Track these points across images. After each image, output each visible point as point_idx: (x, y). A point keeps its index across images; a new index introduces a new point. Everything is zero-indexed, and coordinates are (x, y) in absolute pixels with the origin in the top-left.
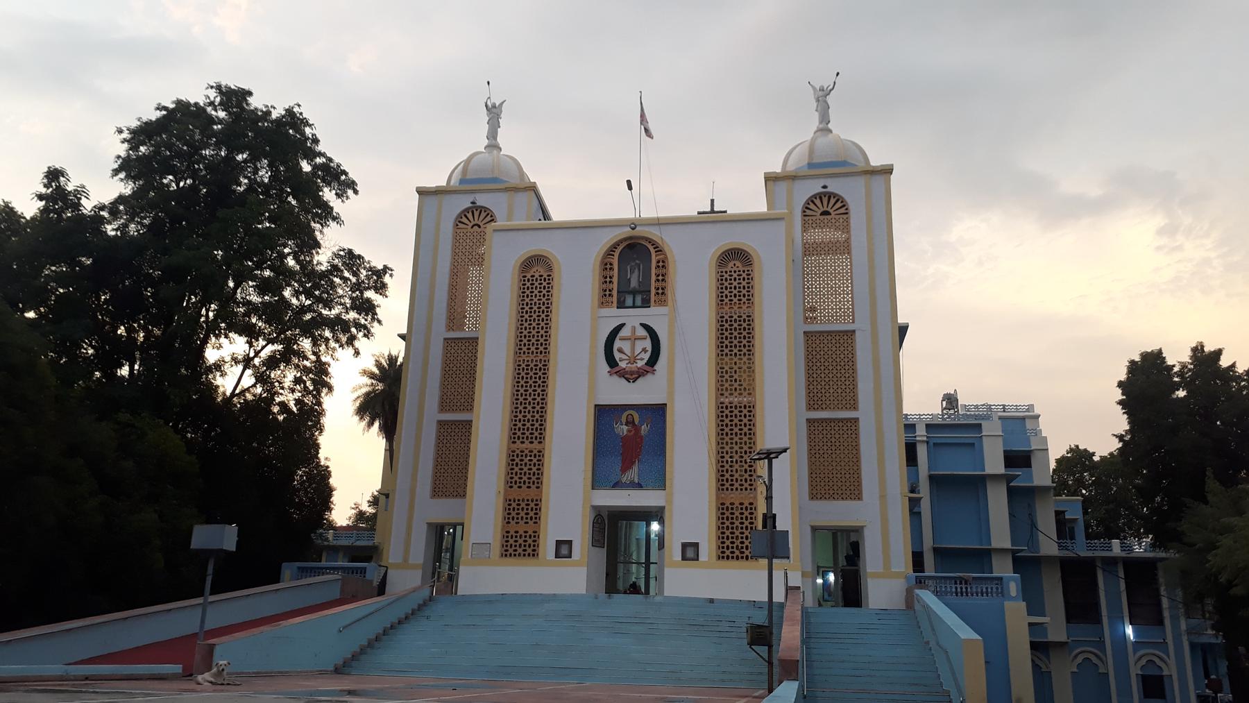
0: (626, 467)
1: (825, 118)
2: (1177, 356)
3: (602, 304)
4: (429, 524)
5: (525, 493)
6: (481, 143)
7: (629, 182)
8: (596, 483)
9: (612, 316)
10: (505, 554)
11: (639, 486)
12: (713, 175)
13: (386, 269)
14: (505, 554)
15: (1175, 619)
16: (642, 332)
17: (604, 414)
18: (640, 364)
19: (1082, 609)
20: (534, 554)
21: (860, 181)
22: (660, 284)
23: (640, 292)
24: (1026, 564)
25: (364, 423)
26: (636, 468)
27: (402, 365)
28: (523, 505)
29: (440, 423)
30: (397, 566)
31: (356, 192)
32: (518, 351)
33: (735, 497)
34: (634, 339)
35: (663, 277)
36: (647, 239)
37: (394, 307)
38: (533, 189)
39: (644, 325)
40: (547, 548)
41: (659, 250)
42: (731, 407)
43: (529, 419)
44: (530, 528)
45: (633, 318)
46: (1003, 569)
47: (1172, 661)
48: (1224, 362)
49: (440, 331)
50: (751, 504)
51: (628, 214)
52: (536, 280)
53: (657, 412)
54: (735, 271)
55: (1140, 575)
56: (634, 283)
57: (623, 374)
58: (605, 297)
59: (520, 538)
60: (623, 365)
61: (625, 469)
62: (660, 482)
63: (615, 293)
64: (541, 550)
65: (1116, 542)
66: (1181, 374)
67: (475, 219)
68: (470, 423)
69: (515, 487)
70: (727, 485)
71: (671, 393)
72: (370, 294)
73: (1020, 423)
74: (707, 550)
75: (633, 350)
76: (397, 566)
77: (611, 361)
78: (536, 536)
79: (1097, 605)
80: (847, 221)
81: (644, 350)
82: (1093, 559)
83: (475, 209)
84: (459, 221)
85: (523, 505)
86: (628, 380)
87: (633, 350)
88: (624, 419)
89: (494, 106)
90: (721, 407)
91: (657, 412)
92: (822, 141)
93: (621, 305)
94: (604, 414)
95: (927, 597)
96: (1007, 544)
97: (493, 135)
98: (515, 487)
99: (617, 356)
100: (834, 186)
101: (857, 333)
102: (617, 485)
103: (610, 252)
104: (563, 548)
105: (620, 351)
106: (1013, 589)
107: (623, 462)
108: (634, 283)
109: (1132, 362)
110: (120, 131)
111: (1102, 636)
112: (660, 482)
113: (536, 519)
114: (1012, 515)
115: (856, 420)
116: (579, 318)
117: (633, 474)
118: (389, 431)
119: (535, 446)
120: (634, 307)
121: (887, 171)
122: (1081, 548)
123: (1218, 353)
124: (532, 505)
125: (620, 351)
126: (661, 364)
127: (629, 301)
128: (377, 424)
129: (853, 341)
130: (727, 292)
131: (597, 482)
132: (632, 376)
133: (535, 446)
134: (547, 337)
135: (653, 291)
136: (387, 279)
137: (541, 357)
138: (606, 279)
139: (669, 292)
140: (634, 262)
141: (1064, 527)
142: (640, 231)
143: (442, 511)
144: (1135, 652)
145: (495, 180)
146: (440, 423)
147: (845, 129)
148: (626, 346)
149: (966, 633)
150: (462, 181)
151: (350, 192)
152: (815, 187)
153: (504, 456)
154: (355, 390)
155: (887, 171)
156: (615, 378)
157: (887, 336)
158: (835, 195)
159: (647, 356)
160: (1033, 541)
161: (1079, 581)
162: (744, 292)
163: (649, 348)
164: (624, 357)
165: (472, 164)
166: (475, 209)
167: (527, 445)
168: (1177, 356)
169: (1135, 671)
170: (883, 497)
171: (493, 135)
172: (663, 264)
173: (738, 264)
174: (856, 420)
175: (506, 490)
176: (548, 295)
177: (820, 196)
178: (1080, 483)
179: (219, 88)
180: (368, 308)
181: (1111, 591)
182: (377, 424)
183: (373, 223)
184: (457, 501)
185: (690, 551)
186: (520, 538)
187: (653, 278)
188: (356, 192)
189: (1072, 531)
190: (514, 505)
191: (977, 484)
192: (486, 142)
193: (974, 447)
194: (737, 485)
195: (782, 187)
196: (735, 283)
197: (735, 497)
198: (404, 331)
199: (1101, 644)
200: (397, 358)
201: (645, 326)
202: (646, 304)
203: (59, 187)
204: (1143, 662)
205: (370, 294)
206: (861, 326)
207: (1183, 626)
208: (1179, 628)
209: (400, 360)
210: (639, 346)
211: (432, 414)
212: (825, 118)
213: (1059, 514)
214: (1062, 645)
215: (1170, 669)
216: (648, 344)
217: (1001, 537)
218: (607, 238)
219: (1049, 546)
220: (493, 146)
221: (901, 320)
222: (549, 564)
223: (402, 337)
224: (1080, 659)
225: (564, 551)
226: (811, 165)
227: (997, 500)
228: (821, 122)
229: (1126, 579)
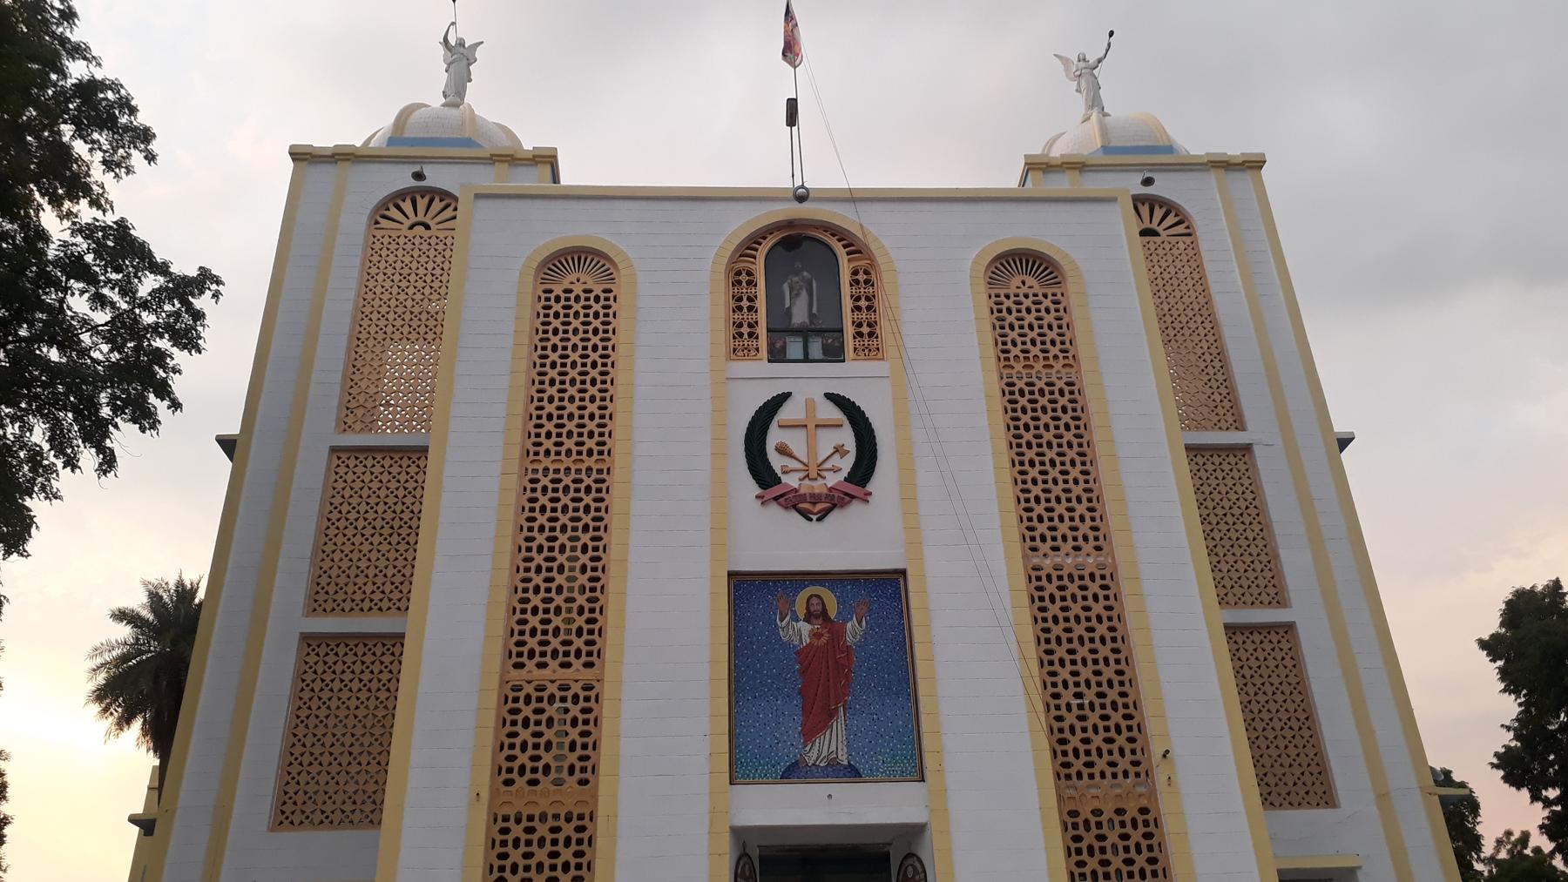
0: (813, 727)
5: (549, 798)
6: (432, 96)
7: (792, 106)
9: (759, 379)
11: (852, 773)
16: (833, 413)
17: (752, 594)
18: (832, 480)
22: (864, 315)
23: (820, 332)
25: (110, 721)
26: (839, 725)
27: (201, 603)
28: (543, 830)
29: (307, 639)
31: (151, 158)
32: (534, 449)
35: (867, 303)
37: (214, 377)
39: (832, 397)
41: (855, 247)
45: (808, 383)
49: (322, 431)
50: (1144, 811)
51: (779, 178)
52: (576, 309)
53: (884, 591)
56: (799, 316)
57: (794, 502)
58: (741, 338)
61: (809, 734)
63: (762, 330)
69: (521, 782)
70: (1078, 765)
71: (914, 542)
75: (812, 448)
77: (762, 473)
80: (1194, 245)
81: (839, 450)
85: (543, 830)
86: (806, 515)
87: (812, 448)
88: (800, 608)
90: (1036, 577)
91: (884, 591)
93: (777, 355)
94: (752, 594)
98: (521, 782)
99: (776, 461)
101: (1257, 450)
102: (794, 772)
103: (750, 245)
105: (783, 450)
107: (807, 710)
112: (907, 759)
115: (1289, 628)
116: (679, 385)
117: (833, 743)
118: (162, 738)
119: (577, 673)
120: (806, 359)
124: (568, 829)
125: (783, 450)
126: (883, 479)
127: (795, 348)
128: (137, 724)
129: (1251, 468)
131: (746, 761)
132: (815, 507)
133: (577, 673)
134: (605, 417)
135: (849, 330)
136: (202, 302)
137: (590, 462)
138: (741, 303)
139: (884, 328)
140: (802, 272)
145: (467, 142)
151: (137, 158)
153: (493, 700)
154: (97, 651)
156: (775, 510)
158: (1162, 202)
159: (847, 463)
164: (793, 464)
165: (417, 116)
167: (553, 670)
172: (866, 278)
173: (1030, 281)
175: (494, 793)
182: (137, 724)
187: (847, 304)
188: (151, 158)
190: (517, 831)
194: (1101, 764)
197: (1101, 795)
198: (233, 428)
200: (193, 592)
201: (832, 397)
202: (834, 354)
209: (201, 595)
210: (827, 442)
216: (847, 437)
218: (741, 222)
221: (1340, 426)
226: (1106, 149)
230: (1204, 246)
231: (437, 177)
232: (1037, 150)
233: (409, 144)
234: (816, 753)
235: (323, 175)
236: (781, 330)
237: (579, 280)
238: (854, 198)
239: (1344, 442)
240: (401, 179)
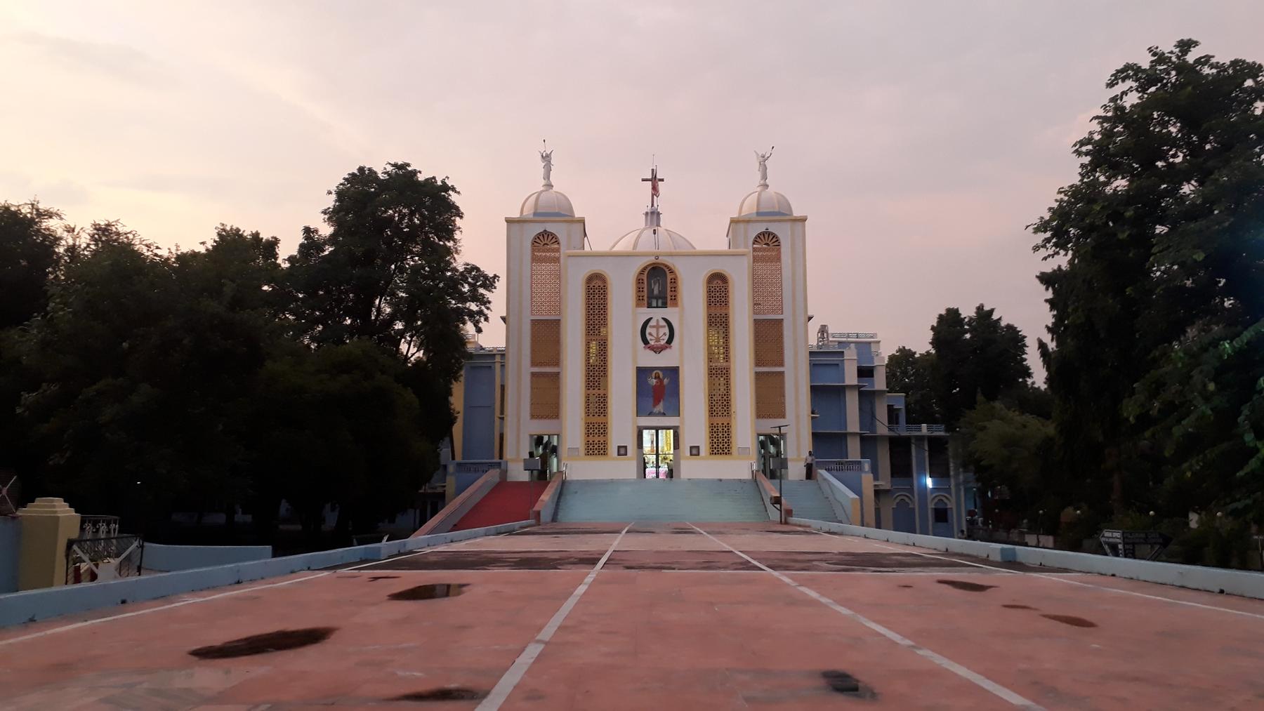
1: (764, 177)
2: (968, 312)
3: (638, 305)
4: (531, 436)
6: (539, 185)
8: (640, 412)
9: (645, 313)
10: (587, 454)
11: (664, 414)
12: (702, 226)
13: (495, 276)
14: (587, 454)
15: (957, 475)
16: (664, 323)
17: (642, 373)
18: (663, 342)
19: (901, 469)
20: (605, 454)
21: (788, 225)
24: (868, 442)
29: (533, 374)
30: (513, 460)
33: (719, 420)
34: (658, 327)
37: (498, 299)
38: (582, 221)
40: (613, 450)
41: (672, 272)
42: (717, 369)
43: (596, 375)
44: (602, 439)
45: (657, 314)
46: (854, 448)
47: (953, 499)
48: (995, 317)
51: (653, 250)
52: (596, 289)
53: (674, 372)
54: (718, 286)
55: (937, 446)
56: (656, 292)
58: (639, 301)
59: (596, 445)
60: (652, 343)
62: (677, 413)
64: (609, 451)
66: (969, 324)
67: (545, 240)
68: (558, 374)
72: (481, 291)
73: (865, 347)
74: (704, 450)
75: (658, 334)
76: (513, 460)
78: (605, 443)
79: (909, 466)
82: (908, 439)
83: (545, 234)
84: (534, 242)
87: (658, 334)
91: (674, 372)
92: (765, 195)
93: (649, 306)
94: (642, 373)
95: (823, 472)
96: (858, 431)
97: (547, 176)
99: (649, 337)
100: (773, 228)
102: (651, 414)
103: (642, 272)
104: (622, 451)
106: (867, 467)
108: (656, 292)
109: (941, 316)
110: (330, 193)
111: (912, 485)
112: (677, 413)
113: (605, 433)
114: (860, 409)
115: (782, 373)
116: (624, 313)
117: (660, 408)
121: (803, 220)
122: (903, 431)
123: (992, 311)
127: (654, 304)
132: (658, 350)
138: (639, 290)
139: (679, 298)
140: (657, 283)
141: (893, 414)
142: (662, 260)
143: (540, 427)
146: (533, 374)
147: (776, 186)
149: (853, 495)
150: (535, 214)
152: (761, 228)
155: (803, 220)
157: (802, 319)
159: (666, 338)
160: (872, 426)
161: (900, 448)
166: (545, 234)
167: (597, 391)
168: (968, 312)
169: (931, 506)
170: (797, 417)
171: (547, 176)
172: (674, 281)
174: (782, 373)
176: (605, 299)
177: (763, 234)
178: (905, 373)
179: (395, 165)
180: (485, 302)
181: (918, 456)
183: (479, 243)
184: (555, 421)
185: (695, 451)
186: (596, 445)
189: (897, 418)
191: (840, 391)
192: (543, 182)
193: (838, 366)
195: (742, 226)
197: (719, 420)
199: (911, 490)
202: (664, 305)
203: (312, 238)
205: (481, 291)
206: (787, 316)
207: (961, 477)
208: (958, 477)
211: (527, 369)
212: (764, 177)
213: (890, 408)
214: (888, 491)
215: (951, 504)
216: (667, 330)
217: (853, 425)
219: (882, 429)
220: (549, 186)
221: (810, 314)
222: (614, 459)
223: (504, 319)
225: (622, 451)
226: (758, 214)
227: (852, 401)
229: (930, 450)
230: (783, 250)
231: (551, 228)
232: (735, 215)
233: (540, 215)
234: (656, 410)
235: (516, 227)
236: (651, 296)
238: (671, 255)
239: (810, 318)
240: (539, 229)
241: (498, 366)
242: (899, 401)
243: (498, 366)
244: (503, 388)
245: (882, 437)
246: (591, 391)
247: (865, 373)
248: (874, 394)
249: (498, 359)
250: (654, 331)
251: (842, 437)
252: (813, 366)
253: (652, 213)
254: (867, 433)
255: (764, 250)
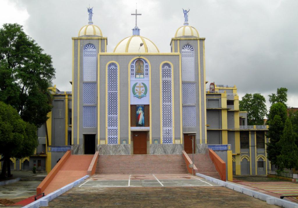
16: (142, 85)
19: (245, 144)
24: (231, 133)
36: (144, 60)
39: (143, 83)
46: (225, 136)
63: (134, 74)
65: (255, 126)
70: (165, 125)
77: (134, 93)
79: (248, 143)
86: (139, 98)
89: (91, 10)
99: (136, 92)
105: (137, 90)
106: (229, 148)
122: (246, 127)
125: (137, 90)
130: (164, 75)
132: (140, 97)
135: (145, 74)
141: (242, 120)
144: (257, 156)
148: (138, 89)
159: (144, 92)
161: (244, 134)
162: (169, 75)
163: (144, 89)
164: (138, 92)
173: (167, 67)
181: (252, 140)
189: (244, 122)
191: (219, 111)
192: (88, 21)
193: (218, 101)
194: (167, 125)
196: (167, 72)
198: (71, 81)
201: (143, 83)
204: (259, 158)
210: (142, 89)
213: (240, 118)
216: (144, 88)
217: (225, 126)
219: (237, 126)
224: (243, 158)
227: (224, 115)
228: (185, 21)
237: (113, 67)
241: (67, 100)
242: (244, 114)
243: (67, 100)
244: (70, 111)
245: (237, 131)
246: (110, 115)
247: (230, 103)
248: (234, 112)
249: (67, 97)
250: (138, 89)
251: (220, 132)
252: (208, 100)
253: (136, 29)
254: (231, 130)
255: (187, 52)
